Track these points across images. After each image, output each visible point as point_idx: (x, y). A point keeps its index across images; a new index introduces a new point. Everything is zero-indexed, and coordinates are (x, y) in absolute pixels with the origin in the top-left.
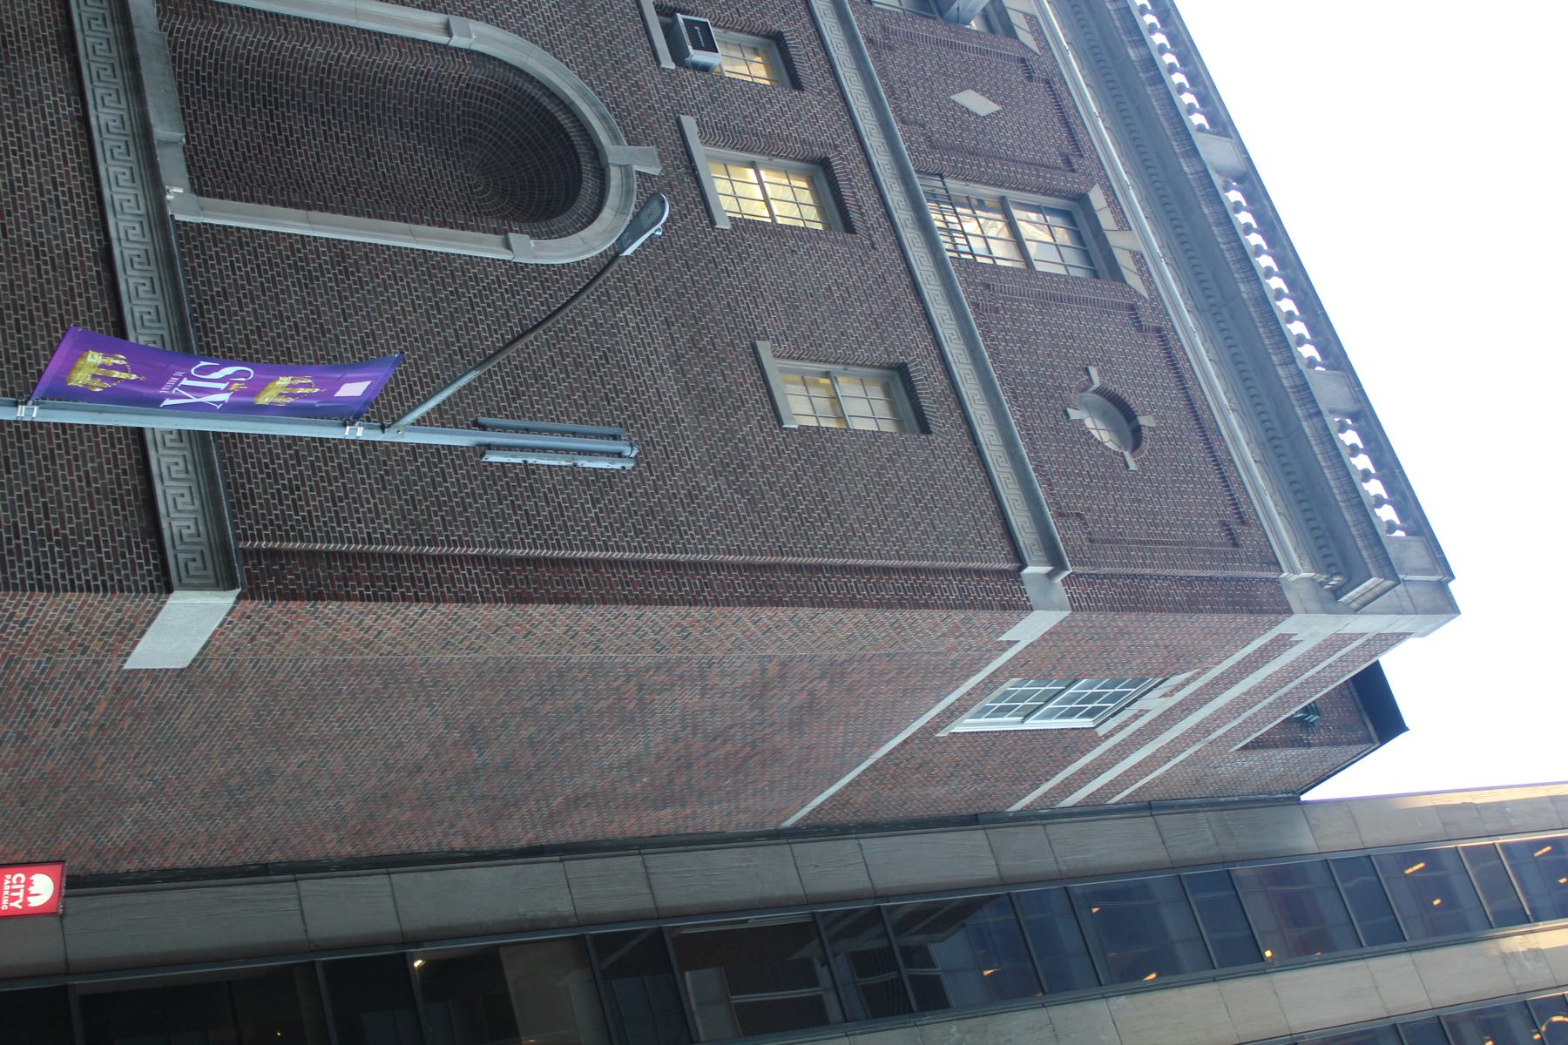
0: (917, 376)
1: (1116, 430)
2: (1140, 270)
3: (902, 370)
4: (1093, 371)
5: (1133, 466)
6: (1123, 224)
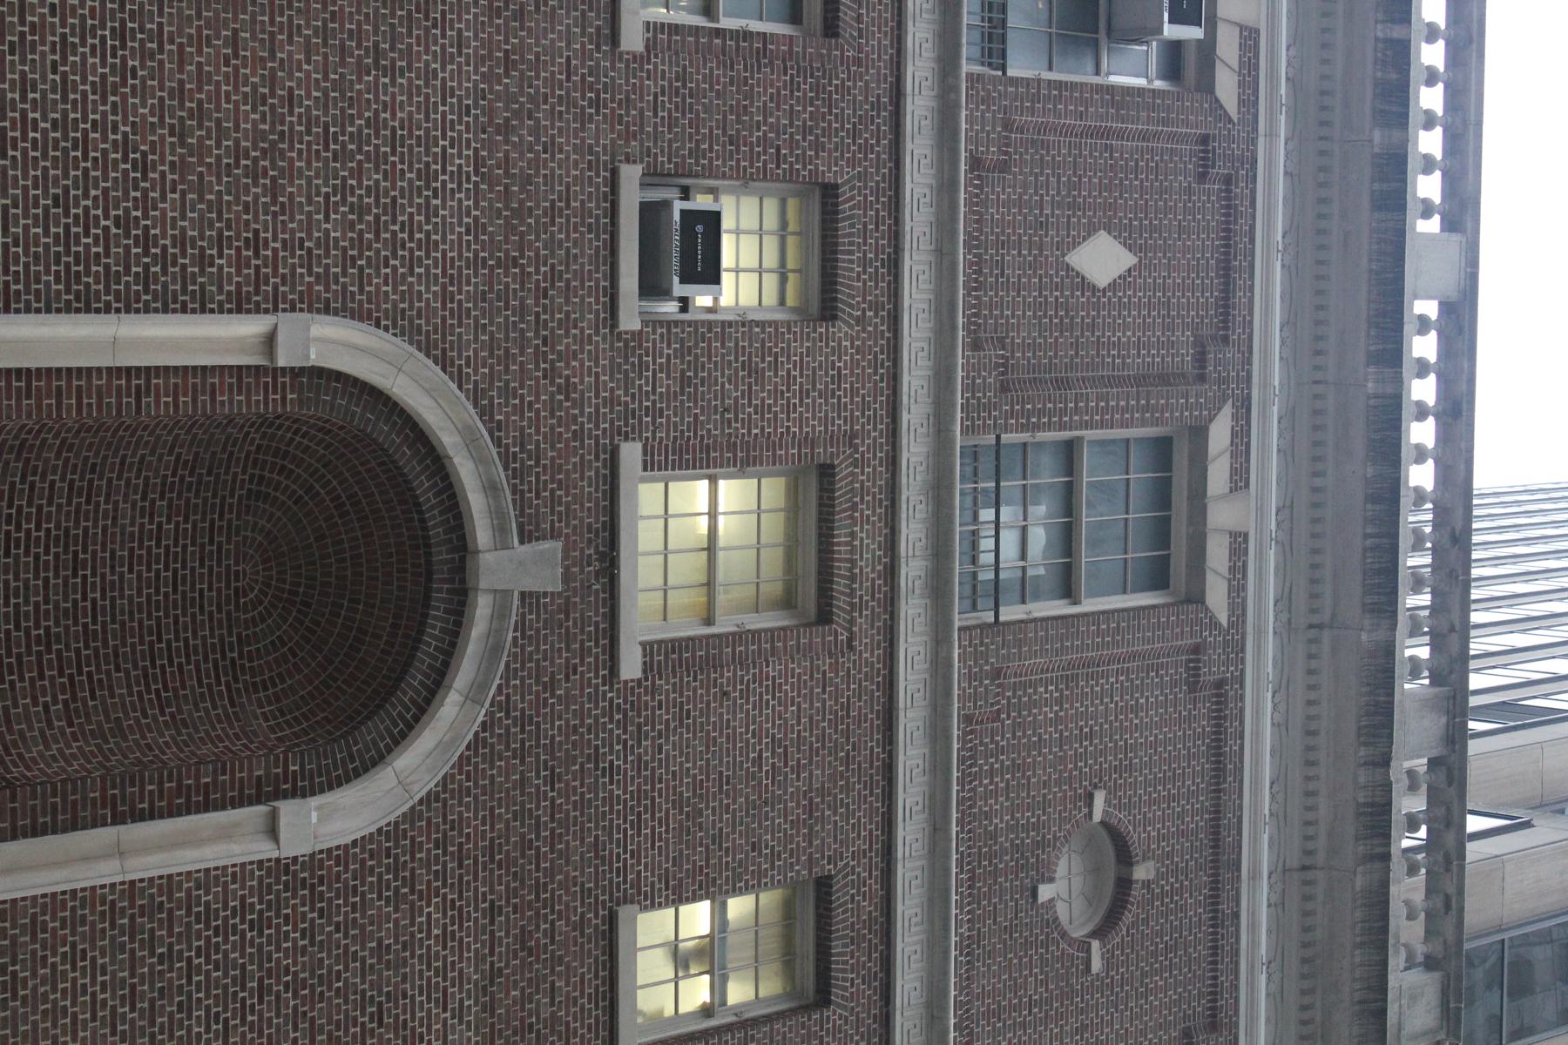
0: (839, 897)
1: (1095, 871)
2: (1232, 569)
3: (823, 886)
4: (1099, 799)
5: (1096, 965)
6: (1240, 479)
